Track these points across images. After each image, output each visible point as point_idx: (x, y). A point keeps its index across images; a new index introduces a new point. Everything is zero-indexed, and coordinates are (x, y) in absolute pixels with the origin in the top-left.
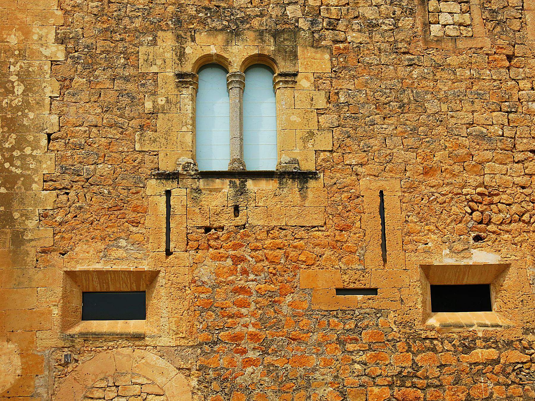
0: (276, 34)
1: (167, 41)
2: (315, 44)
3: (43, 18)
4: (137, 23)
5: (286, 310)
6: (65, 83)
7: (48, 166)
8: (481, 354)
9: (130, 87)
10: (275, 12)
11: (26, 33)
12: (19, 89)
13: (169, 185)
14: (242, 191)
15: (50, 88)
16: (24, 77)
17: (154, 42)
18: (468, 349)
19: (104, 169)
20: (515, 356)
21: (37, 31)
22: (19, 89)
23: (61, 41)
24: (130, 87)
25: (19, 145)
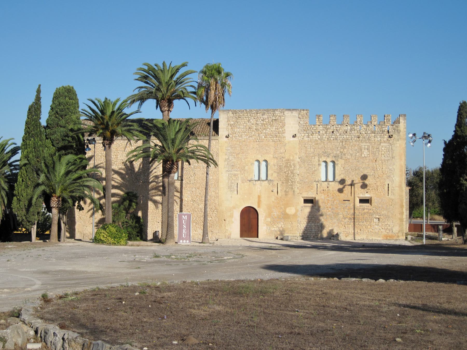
0: (335, 157)
1: (317, 158)
2: (341, 158)
3: (296, 154)
4: (311, 155)
5: (335, 203)
6: (300, 166)
7: (298, 180)
8: (366, 211)
9: (311, 166)
10: (335, 152)
11: (294, 157)
12: (293, 167)
13: (317, 183)
14: (329, 184)
15: (298, 167)
16: (294, 164)
17: (314, 158)
18: (364, 210)
19: (307, 180)
20: (371, 211)
21: (295, 156)
22: (293, 167)
23: (299, 158)
24: (311, 166)
25: (293, 176)
